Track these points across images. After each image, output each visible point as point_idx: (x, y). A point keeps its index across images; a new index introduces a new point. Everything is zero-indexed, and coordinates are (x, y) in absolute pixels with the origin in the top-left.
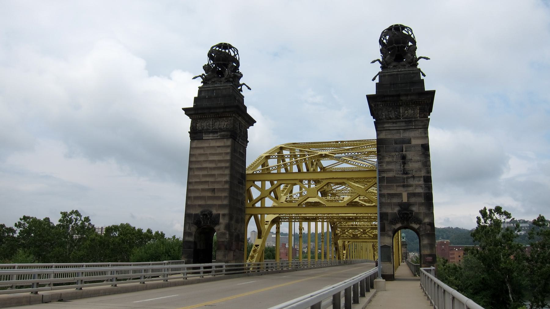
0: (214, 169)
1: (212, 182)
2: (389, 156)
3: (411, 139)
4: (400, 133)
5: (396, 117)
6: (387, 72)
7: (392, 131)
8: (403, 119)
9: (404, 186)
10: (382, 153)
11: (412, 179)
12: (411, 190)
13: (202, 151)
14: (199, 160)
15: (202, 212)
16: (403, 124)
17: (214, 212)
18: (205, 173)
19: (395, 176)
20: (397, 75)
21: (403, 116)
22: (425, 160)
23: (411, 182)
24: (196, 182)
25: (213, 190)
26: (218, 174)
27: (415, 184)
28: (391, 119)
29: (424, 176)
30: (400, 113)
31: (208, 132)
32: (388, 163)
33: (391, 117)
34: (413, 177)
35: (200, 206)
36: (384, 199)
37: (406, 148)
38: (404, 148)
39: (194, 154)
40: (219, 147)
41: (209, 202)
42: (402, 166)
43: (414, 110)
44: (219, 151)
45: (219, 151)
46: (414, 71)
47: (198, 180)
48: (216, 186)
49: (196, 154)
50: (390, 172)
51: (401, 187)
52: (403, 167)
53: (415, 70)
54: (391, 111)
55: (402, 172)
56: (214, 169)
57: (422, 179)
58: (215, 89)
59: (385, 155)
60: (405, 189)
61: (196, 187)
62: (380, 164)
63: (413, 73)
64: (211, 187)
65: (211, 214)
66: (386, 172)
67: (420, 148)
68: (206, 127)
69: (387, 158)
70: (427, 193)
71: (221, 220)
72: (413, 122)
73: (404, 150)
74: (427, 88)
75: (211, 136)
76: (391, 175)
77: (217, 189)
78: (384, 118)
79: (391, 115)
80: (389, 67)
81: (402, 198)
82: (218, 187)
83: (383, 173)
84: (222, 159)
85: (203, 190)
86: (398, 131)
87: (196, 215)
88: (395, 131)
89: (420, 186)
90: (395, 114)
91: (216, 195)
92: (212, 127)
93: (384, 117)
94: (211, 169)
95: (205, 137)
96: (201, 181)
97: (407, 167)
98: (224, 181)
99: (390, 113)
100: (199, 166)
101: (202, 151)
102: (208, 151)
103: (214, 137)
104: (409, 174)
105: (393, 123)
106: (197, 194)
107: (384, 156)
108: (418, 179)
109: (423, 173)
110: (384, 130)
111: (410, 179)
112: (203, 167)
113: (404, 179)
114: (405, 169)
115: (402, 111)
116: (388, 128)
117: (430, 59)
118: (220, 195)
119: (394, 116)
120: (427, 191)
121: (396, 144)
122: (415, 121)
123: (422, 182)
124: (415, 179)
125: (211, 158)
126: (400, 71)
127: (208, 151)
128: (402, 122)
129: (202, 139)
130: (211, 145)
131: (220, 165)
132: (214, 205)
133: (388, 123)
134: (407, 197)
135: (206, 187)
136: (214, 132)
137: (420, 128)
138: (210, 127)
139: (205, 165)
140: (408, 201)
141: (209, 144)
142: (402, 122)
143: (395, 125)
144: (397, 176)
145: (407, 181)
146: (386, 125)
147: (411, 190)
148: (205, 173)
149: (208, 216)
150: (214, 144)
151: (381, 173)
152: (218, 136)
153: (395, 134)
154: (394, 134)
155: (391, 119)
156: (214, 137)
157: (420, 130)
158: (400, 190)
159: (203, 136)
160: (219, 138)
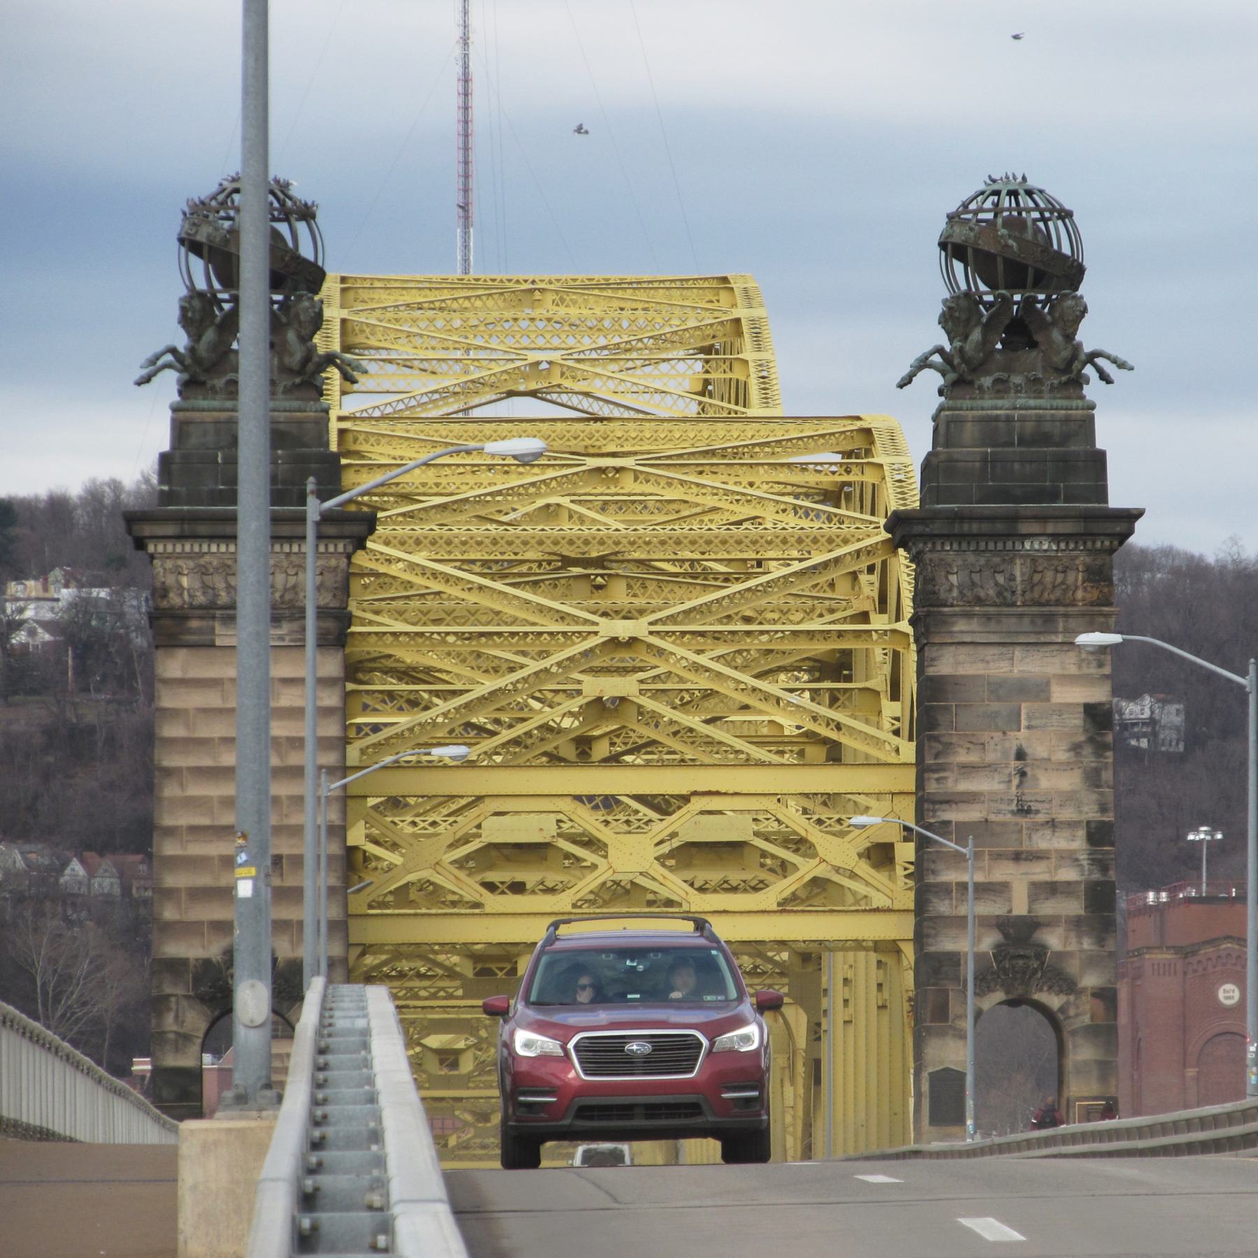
3: (1048, 684)
4: (1012, 659)
5: (999, 594)
9: (1017, 857)
12: (1040, 872)
28: (979, 601)
37: (1029, 718)
60: (1025, 867)
62: (936, 776)
67: (1077, 720)
70: (1097, 883)
76: (972, 814)
79: (982, 587)
89: (1069, 858)
93: (955, 593)
122: (1066, 616)
124: (1057, 834)
143: (993, 626)
147: (1040, 872)
151: (937, 807)
153: (994, 661)
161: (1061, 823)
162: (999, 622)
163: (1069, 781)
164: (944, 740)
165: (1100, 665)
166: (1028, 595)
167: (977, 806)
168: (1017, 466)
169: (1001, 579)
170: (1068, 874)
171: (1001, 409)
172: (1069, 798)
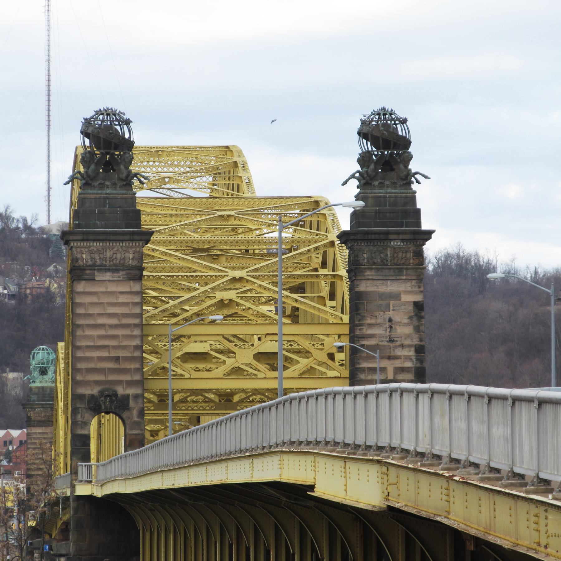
0: (116, 326)
1: (114, 347)
2: (371, 317)
3: (400, 294)
5: (382, 261)
6: (371, 193)
7: (376, 282)
8: (391, 265)
9: (389, 358)
10: (362, 312)
11: (401, 349)
13: (94, 299)
14: (91, 311)
15: (101, 392)
16: (392, 273)
17: (120, 391)
18: (102, 332)
19: (378, 344)
20: (385, 197)
21: (391, 261)
22: (417, 324)
23: (399, 352)
24: (88, 347)
25: (117, 359)
26: (123, 335)
27: (404, 356)
28: (374, 264)
29: (415, 345)
30: (387, 255)
31: (104, 268)
32: (371, 326)
33: (376, 261)
34: (402, 346)
35: (97, 383)
36: (364, 374)
37: (393, 307)
38: (391, 306)
39: (81, 303)
40: (122, 293)
41: (112, 377)
42: (388, 330)
43: (406, 253)
44: (122, 299)
45: (122, 299)
46: (408, 193)
47: (91, 344)
48: (121, 353)
49: (84, 304)
50: (372, 339)
51: (386, 359)
52: (390, 332)
53: (410, 193)
54: (375, 253)
55: (388, 339)
56: (116, 326)
57: (413, 349)
58: (108, 198)
59: (366, 315)
60: (392, 362)
61: (88, 354)
62: (359, 328)
63: (406, 197)
64: (113, 354)
65: (116, 394)
66: (367, 338)
67: (411, 308)
68: (100, 261)
69: (368, 318)
70: (419, 368)
71: (132, 403)
72: (405, 271)
73: (391, 308)
74: (425, 226)
75: (108, 276)
76: (372, 342)
77: (123, 357)
78: (365, 263)
80: (373, 184)
81: (387, 374)
82: (125, 355)
83: (362, 339)
84: (128, 312)
85: (101, 359)
86: (383, 281)
87: (92, 396)
88: (380, 282)
89: (408, 358)
90: (381, 257)
91: (123, 366)
92: (110, 261)
93: (366, 261)
94: (111, 326)
95: (99, 276)
96: (96, 345)
97: (393, 334)
98: (134, 346)
99: (373, 255)
100: (92, 322)
101: (94, 299)
102: (105, 300)
103: (113, 277)
104: (397, 341)
105: (378, 270)
106: (91, 365)
107: (364, 316)
108: (407, 349)
109: (416, 342)
110: (365, 279)
111: (397, 349)
112: (98, 323)
113: (390, 348)
114: (391, 335)
115: (390, 254)
116: (370, 277)
117: (429, 178)
118: (128, 367)
119: (379, 260)
120: (419, 365)
121: (382, 300)
122: (407, 269)
123: (411, 353)
124: (404, 349)
125: (111, 310)
126: (389, 193)
127: (105, 300)
128: (390, 269)
129: (94, 280)
130: (109, 290)
131: (124, 321)
132: (120, 382)
133: (371, 269)
134: (394, 373)
135: (105, 354)
136: (114, 269)
137: (414, 279)
138: (106, 261)
139: (101, 321)
140: (394, 378)
141: (106, 288)
142: (390, 269)
144: (380, 343)
145: (394, 351)
146: (368, 273)
147: (398, 363)
148: (102, 332)
149: (114, 398)
150: (112, 288)
151: (360, 339)
152: (119, 277)
154: (378, 286)
155: (374, 264)
156: (113, 277)
157: (414, 281)
158: (385, 363)
159: (96, 275)
160: (121, 279)
161: (406, 345)
162: (382, 271)
163: (408, 330)
164: (363, 314)
165: (419, 287)
166: (392, 262)
167: (374, 339)
168: (388, 214)
169: (382, 255)
170: (408, 364)
171: (382, 193)
172: (408, 336)
